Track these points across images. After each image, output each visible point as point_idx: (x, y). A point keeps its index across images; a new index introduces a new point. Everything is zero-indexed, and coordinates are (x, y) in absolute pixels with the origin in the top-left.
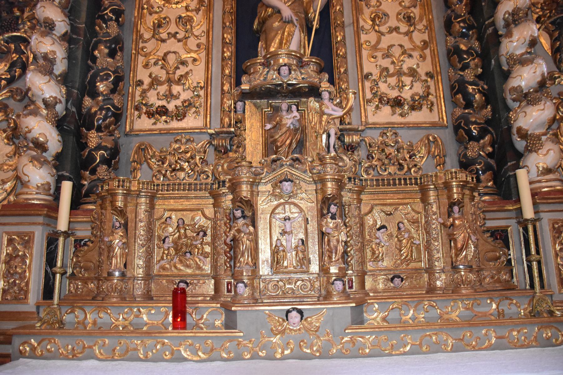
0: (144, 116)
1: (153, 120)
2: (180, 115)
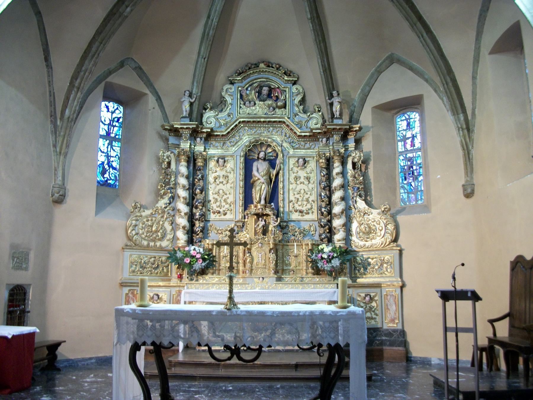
0: (212, 214)
1: (215, 215)
2: (225, 214)
